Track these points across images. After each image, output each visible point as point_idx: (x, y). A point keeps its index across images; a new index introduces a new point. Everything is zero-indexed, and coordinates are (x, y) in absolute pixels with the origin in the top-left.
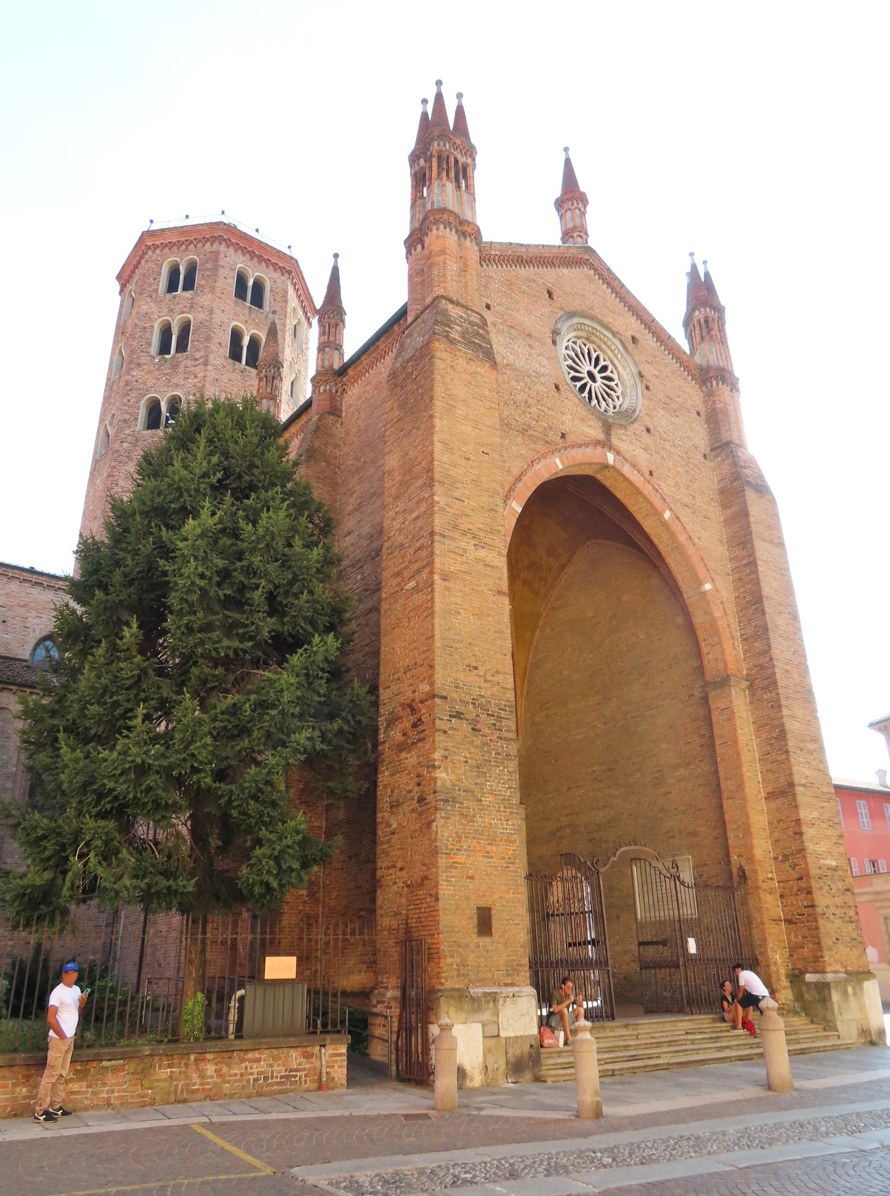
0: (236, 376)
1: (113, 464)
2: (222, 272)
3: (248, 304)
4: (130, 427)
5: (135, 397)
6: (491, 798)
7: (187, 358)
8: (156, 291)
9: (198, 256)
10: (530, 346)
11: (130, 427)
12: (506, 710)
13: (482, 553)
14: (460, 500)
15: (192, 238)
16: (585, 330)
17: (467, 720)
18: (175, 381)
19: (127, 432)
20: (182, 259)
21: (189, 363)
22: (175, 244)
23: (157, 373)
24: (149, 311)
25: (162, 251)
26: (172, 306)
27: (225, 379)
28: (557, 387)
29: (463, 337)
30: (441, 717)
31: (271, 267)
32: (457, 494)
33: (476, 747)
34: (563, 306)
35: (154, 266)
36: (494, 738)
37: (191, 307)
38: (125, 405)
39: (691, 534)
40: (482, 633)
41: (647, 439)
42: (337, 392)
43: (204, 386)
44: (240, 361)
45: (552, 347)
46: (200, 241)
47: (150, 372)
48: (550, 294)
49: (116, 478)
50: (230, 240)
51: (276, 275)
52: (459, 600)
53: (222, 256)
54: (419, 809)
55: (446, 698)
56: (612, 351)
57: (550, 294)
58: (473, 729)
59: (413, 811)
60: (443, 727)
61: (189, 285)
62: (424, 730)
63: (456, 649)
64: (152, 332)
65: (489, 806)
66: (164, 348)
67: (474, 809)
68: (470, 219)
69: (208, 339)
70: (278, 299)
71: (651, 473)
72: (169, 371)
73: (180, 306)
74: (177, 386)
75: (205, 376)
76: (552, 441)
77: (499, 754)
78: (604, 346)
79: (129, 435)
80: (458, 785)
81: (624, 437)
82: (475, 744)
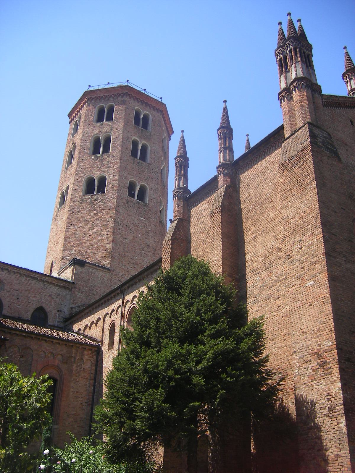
3: (141, 128)
10: (347, 150)
15: (111, 94)
20: (106, 105)
22: (102, 97)
29: (323, 145)
31: (152, 108)
37: (111, 130)
42: (233, 174)
44: (137, 157)
46: (116, 95)
50: (131, 95)
51: (155, 113)
54: (330, 415)
59: (325, 416)
62: (330, 368)
68: (315, 82)
79: (78, 198)
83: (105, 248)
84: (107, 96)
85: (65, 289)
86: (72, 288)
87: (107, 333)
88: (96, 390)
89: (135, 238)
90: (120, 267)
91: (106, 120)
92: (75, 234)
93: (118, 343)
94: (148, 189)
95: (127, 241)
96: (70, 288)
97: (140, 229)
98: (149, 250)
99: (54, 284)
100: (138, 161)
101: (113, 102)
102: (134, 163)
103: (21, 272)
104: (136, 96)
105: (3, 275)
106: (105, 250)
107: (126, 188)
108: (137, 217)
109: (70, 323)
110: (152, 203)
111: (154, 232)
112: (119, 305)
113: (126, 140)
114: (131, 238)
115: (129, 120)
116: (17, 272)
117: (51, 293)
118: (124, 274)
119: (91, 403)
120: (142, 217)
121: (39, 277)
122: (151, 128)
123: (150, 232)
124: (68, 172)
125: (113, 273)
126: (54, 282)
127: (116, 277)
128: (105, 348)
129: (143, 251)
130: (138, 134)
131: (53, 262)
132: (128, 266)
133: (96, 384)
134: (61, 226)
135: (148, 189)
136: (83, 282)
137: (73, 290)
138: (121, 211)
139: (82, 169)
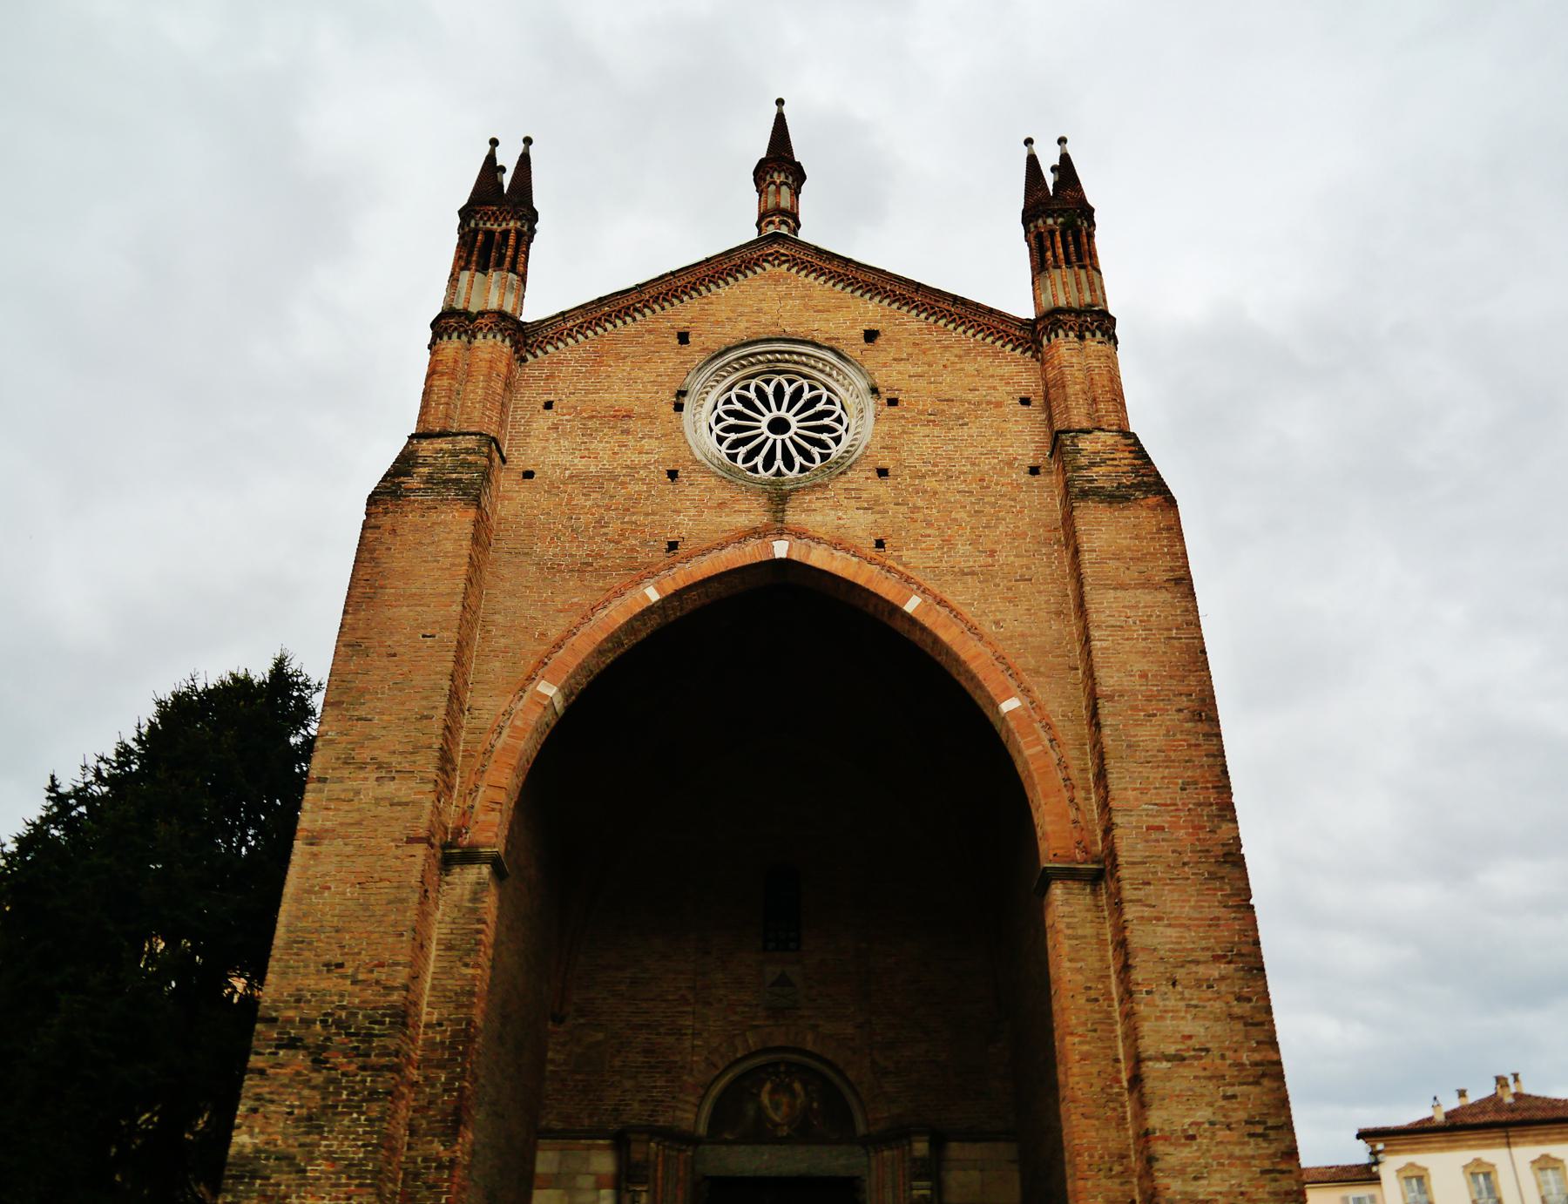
6: (324, 1166)
12: (382, 1023)
13: (389, 788)
14: (366, 720)
16: (761, 362)
17: (306, 1048)
28: (673, 475)
30: (262, 1051)
32: (362, 713)
33: (314, 1088)
34: (708, 344)
36: (353, 1068)
39: (975, 621)
40: (366, 910)
41: (881, 489)
45: (674, 415)
48: (683, 338)
52: (332, 868)
55: (275, 1020)
56: (822, 371)
57: (683, 338)
58: (315, 1061)
60: (261, 1065)
63: (310, 943)
65: (318, 1179)
67: (288, 1186)
71: (880, 544)
76: (642, 563)
77: (355, 1094)
78: (806, 370)
80: (265, 1151)
81: (818, 505)
82: (314, 1082)
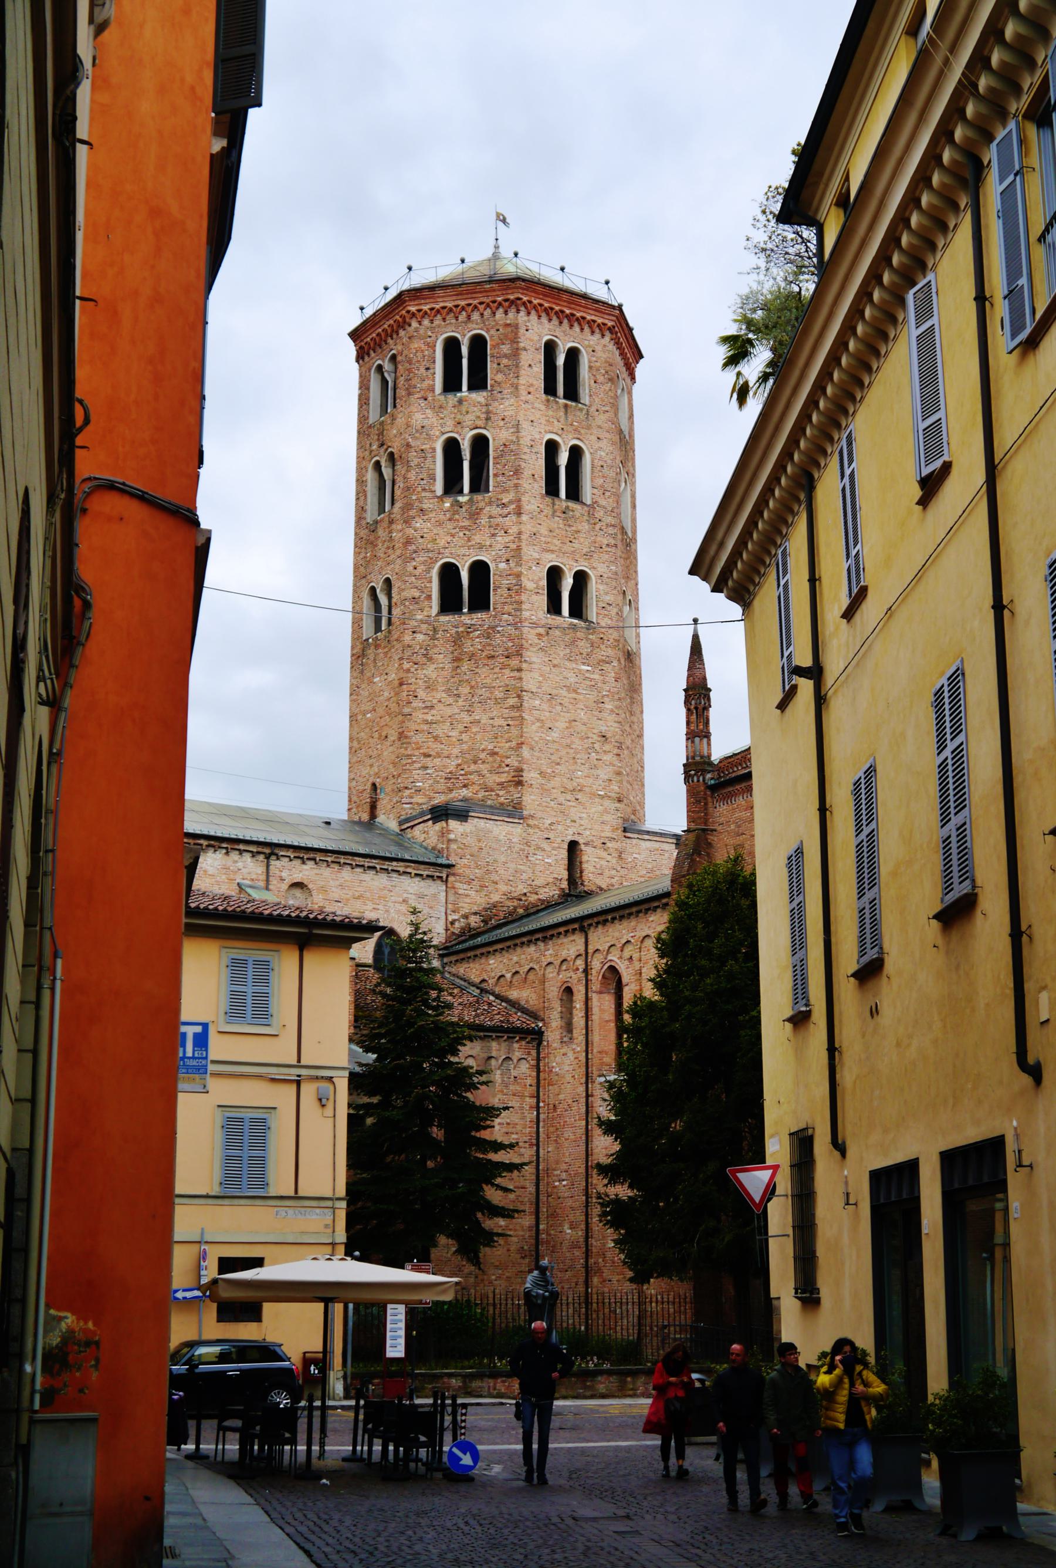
0: (558, 522)
1: (406, 666)
2: (525, 358)
4: (422, 610)
5: (424, 563)
7: (490, 503)
8: (432, 389)
9: (488, 331)
11: (422, 610)
15: (475, 302)
18: (477, 538)
19: (419, 617)
21: (495, 510)
23: (450, 525)
24: (426, 423)
25: (432, 321)
26: (459, 416)
27: (543, 530)
31: (587, 329)
35: (423, 346)
37: (488, 419)
38: (411, 575)
43: (519, 549)
46: (488, 306)
47: (440, 524)
49: (413, 687)
50: (530, 302)
53: (522, 331)
61: (478, 382)
64: (434, 457)
66: (452, 484)
69: (517, 472)
70: (600, 379)
72: (466, 523)
73: (471, 417)
74: (481, 547)
75: (520, 533)
83: (508, 761)
84: (463, 309)
85: (434, 880)
86: (447, 876)
87: (557, 1006)
88: (542, 1116)
89: (574, 723)
90: (544, 804)
91: (472, 388)
92: (426, 722)
93: (584, 1032)
94: (594, 582)
95: (555, 735)
96: (444, 877)
97: (581, 697)
98: (607, 747)
99: (410, 873)
100: (564, 504)
101: (481, 329)
102: (553, 516)
103: (342, 861)
104: (541, 301)
105: (307, 873)
106: (507, 766)
107: (540, 591)
108: (574, 666)
109: (457, 961)
110: (606, 619)
111: (616, 697)
112: (578, 953)
113: (528, 451)
114: (561, 725)
115: (532, 385)
116: (333, 862)
117: (405, 895)
118: (554, 820)
119: (534, 1141)
120: (584, 664)
121: (378, 864)
122: (587, 391)
123: (606, 699)
124: (381, 532)
125: (531, 822)
126: (409, 870)
127: (537, 830)
128: (553, 1034)
129: (594, 754)
130: (556, 423)
131: (374, 785)
132: (561, 799)
133: (541, 1104)
134: (386, 694)
135: (594, 582)
136: (468, 857)
137: (451, 879)
138: (534, 659)
139: (422, 537)
